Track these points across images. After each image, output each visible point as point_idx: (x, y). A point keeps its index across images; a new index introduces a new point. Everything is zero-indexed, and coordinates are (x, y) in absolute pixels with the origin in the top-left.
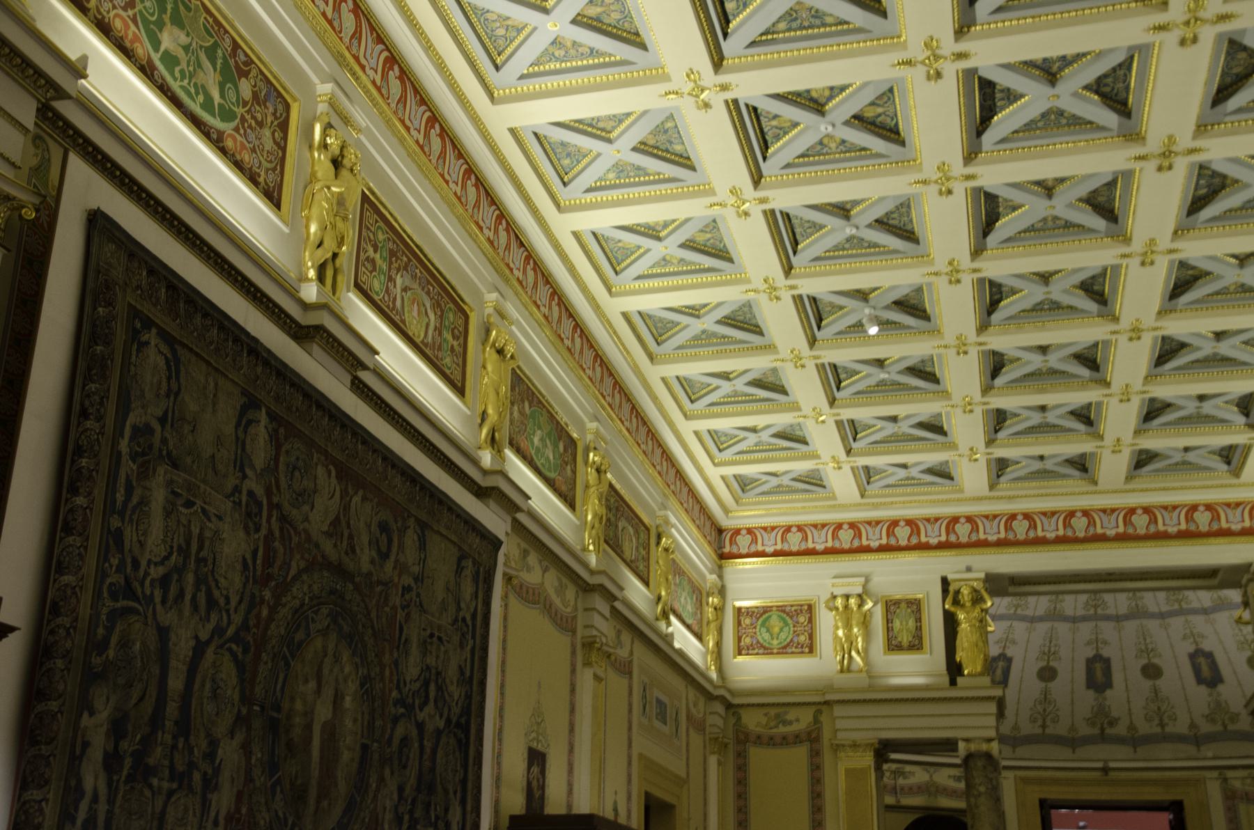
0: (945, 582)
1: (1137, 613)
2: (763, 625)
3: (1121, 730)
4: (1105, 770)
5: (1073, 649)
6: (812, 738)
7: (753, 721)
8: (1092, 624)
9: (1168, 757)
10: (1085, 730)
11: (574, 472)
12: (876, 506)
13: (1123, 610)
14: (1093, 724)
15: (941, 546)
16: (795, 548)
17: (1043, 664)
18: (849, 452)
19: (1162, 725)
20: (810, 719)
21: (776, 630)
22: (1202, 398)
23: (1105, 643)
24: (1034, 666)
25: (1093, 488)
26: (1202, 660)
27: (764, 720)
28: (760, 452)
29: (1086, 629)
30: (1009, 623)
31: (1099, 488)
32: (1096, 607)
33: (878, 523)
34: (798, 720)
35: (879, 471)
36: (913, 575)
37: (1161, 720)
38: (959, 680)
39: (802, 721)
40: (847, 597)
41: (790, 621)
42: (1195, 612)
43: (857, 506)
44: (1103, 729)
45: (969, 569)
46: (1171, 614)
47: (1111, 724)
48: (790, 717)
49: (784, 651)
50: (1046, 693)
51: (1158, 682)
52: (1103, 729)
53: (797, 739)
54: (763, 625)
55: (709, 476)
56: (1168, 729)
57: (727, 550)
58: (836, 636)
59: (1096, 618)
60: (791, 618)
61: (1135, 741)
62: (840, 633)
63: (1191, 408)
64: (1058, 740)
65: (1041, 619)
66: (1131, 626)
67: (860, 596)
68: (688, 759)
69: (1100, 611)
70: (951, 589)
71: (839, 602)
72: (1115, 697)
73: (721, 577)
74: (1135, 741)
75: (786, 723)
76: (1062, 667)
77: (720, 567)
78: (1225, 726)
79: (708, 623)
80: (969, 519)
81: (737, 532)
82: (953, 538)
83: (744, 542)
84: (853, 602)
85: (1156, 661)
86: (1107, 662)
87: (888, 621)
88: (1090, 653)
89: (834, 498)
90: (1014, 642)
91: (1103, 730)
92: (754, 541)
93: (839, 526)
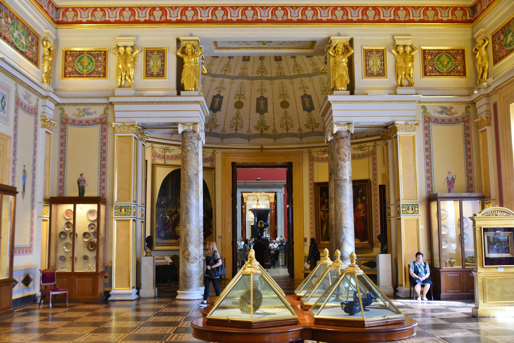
0: (178, 41)
1: (281, 76)
2: (79, 61)
3: (270, 132)
4: (262, 149)
5: (251, 93)
6: (103, 122)
7: (71, 112)
8: (260, 81)
9: (289, 143)
10: (254, 132)
13: (274, 75)
14: (258, 129)
15: (178, 22)
16: (98, 20)
17: (238, 100)
19: (287, 129)
20: (102, 112)
21: (86, 64)
24: (233, 101)
26: (306, 99)
27: (77, 112)
29: (257, 83)
30: (222, 79)
32: (262, 72)
33: (145, 8)
34: (95, 113)
36: (163, 37)
37: (287, 127)
39: (98, 112)
40: (125, 47)
41: (94, 60)
42: (305, 76)
44: (262, 131)
46: (295, 77)
47: (266, 129)
48: (90, 111)
49: (89, 75)
50: (238, 114)
51: (287, 110)
52: (262, 131)
53: (94, 122)
54: (79, 61)
56: (289, 131)
57: (60, 19)
58: (118, 68)
59: (262, 78)
60: (94, 58)
61: (275, 136)
62: (120, 66)
64: (242, 136)
65: (237, 78)
66: (277, 82)
67: (132, 47)
68: (16, 126)
69: (264, 75)
70: (183, 44)
71: (122, 50)
73: (56, 34)
74: (275, 136)
75: (88, 114)
76: (246, 102)
78: (313, 129)
81: (67, 9)
82: (184, 18)
83: (70, 15)
84: (129, 50)
87: (147, 61)
88: (259, 96)
91: (262, 131)
92: (76, 15)
93: (124, 9)
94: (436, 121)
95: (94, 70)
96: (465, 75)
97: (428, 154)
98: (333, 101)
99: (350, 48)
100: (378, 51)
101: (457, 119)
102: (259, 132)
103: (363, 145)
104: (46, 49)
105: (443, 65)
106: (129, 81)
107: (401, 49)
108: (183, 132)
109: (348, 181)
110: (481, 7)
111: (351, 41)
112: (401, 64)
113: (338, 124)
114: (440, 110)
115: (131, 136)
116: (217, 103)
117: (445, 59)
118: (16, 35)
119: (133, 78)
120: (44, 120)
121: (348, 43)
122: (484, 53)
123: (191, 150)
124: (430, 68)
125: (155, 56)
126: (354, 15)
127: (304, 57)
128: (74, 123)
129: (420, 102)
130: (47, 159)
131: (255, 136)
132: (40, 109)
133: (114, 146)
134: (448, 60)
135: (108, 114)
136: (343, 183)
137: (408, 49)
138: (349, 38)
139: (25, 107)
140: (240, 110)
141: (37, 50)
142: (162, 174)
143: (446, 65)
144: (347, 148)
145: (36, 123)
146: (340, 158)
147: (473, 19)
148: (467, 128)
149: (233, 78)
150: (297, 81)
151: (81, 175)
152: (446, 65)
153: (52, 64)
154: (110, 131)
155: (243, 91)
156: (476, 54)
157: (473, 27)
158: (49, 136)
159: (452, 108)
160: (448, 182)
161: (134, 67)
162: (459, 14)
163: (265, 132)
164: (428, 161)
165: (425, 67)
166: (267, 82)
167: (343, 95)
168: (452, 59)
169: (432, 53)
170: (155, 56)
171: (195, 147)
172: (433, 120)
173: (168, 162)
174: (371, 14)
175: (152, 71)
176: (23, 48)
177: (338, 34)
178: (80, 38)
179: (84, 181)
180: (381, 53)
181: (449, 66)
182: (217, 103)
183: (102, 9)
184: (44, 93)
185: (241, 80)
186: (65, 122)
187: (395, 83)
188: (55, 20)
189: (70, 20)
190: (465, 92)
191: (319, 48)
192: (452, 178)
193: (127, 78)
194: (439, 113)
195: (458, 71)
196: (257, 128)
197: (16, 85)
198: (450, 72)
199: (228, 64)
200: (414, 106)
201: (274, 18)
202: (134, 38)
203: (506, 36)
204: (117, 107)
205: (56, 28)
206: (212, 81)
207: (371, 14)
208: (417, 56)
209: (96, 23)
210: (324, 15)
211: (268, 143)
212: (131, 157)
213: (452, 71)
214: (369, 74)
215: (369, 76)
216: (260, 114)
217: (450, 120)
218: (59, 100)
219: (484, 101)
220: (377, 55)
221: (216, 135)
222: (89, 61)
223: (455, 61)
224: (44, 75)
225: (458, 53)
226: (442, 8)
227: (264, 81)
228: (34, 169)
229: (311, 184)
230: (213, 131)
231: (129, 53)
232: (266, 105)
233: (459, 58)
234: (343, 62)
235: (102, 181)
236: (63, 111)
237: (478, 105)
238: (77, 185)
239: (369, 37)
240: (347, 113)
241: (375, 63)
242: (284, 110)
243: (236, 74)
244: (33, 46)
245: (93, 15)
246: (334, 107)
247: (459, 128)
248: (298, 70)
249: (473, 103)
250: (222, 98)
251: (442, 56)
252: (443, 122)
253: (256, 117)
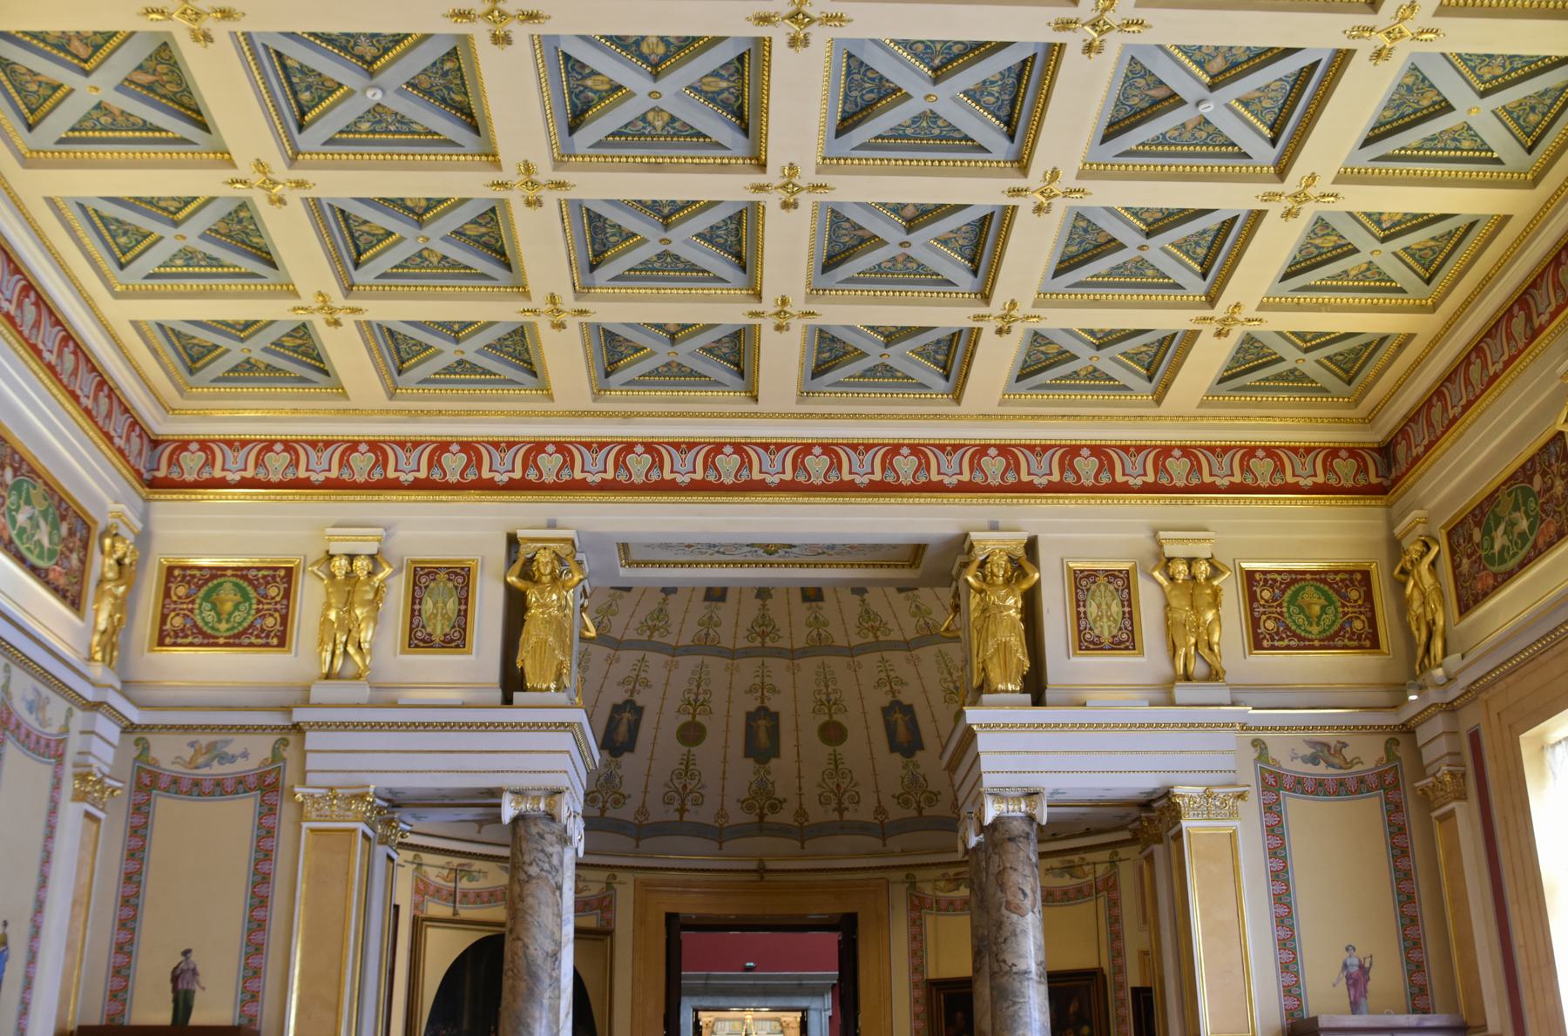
0: (513, 541)
1: (820, 647)
2: (206, 598)
3: (786, 817)
4: (762, 871)
5: (730, 694)
6: (267, 787)
7: (169, 754)
10: (738, 816)
12: (414, 416)
13: (799, 643)
14: (750, 808)
15: (513, 486)
16: (275, 478)
17: (689, 718)
18: (349, 289)
19: (841, 810)
20: (268, 754)
21: (228, 606)
23: (774, 690)
24: (674, 721)
25: (752, 407)
26: (898, 716)
27: (188, 753)
29: (748, 666)
31: (761, 407)
32: (763, 635)
33: (416, 444)
34: (245, 755)
36: (467, 529)
37: (840, 803)
38: (518, 696)
39: (254, 753)
40: (351, 558)
41: (252, 594)
42: (894, 646)
46: (864, 649)
48: (230, 750)
50: (687, 762)
51: (839, 749)
53: (240, 785)
54: (206, 598)
56: (847, 816)
57: (161, 474)
58: (325, 621)
60: (256, 588)
61: (803, 832)
62: (333, 615)
64: (701, 830)
65: (687, 651)
66: (809, 665)
67: (372, 557)
69: (769, 643)
70: (525, 551)
71: (340, 565)
72: (782, 769)
73: (145, 518)
75: (224, 758)
78: (920, 810)
79: (102, 581)
81: (183, 445)
82: (532, 475)
83: (192, 463)
84: (361, 565)
85: (836, 718)
86: (774, 717)
87: (415, 600)
88: (753, 706)
90: (647, 685)
91: (762, 816)
92: (210, 462)
94: (1299, 785)
95: (251, 625)
96: (1375, 645)
97: (1279, 888)
98: (980, 725)
99: (1028, 566)
100: (1111, 575)
101: (1361, 781)
102: (753, 818)
103: (1075, 858)
104: (111, 562)
105: (1308, 618)
106: (357, 659)
107: (1181, 570)
108: (516, 820)
109: (1034, 975)
110: (1409, 448)
111: (1031, 546)
112: (1183, 612)
113: (998, 796)
114: (1309, 751)
115: (354, 830)
116: (623, 728)
117: (1313, 600)
118: (22, 518)
119: (370, 651)
120: (83, 778)
121: (1020, 552)
122: (1428, 580)
123: (538, 877)
124: (1270, 625)
125: (442, 584)
127: (892, 591)
128: (176, 786)
129: (1245, 727)
130: (82, 902)
131: (740, 831)
132: (74, 743)
133: (298, 859)
134: (1323, 601)
135: (284, 760)
136: (1017, 984)
137: (1203, 569)
138: (1023, 536)
139: (28, 735)
140: (694, 750)
141: (83, 562)
142: (443, 949)
143: (1319, 617)
144: (1027, 871)
145: (57, 786)
146: (1008, 903)
147: (1386, 483)
148: (1394, 809)
149: (675, 651)
150: (870, 661)
151: (186, 953)
152: (1319, 617)
153: (125, 606)
154: (287, 812)
155: (705, 692)
156: (1404, 585)
157: (1389, 506)
158: (94, 826)
159: (1345, 745)
160: (1348, 977)
161: (375, 616)
162: (1345, 469)
163: (771, 818)
164: (1283, 911)
165: (1255, 623)
166: (777, 666)
167: (1012, 705)
168: (1335, 597)
169: (1275, 581)
170: (442, 584)
171: (552, 866)
172: (1288, 782)
173: (465, 913)
174: (1087, 467)
175: (429, 630)
176: (40, 556)
177: (992, 526)
178: (215, 530)
179: (194, 972)
180: (1122, 582)
181: (1327, 619)
182: (623, 728)
183: (289, 446)
184: (89, 694)
185: (698, 659)
186: (148, 783)
187: (1166, 668)
188: (146, 476)
190: (1381, 697)
191: (938, 567)
192: (1361, 967)
193: (351, 650)
194: (1305, 760)
195: (1353, 633)
196: (747, 805)
197: (7, 669)
198: (1331, 638)
199: (661, 610)
200: (1228, 739)
201: (802, 478)
202: (380, 531)
203: (1488, 532)
204: (313, 739)
205: (147, 500)
206: (610, 661)
207: (1087, 467)
208: (1231, 590)
209: (268, 485)
210: (949, 470)
211: (780, 854)
212: (347, 897)
213: (1336, 634)
214: (1086, 642)
215: (1088, 649)
216: (758, 761)
217: (1341, 783)
218: (135, 716)
219: (1439, 724)
220: (1111, 587)
221: (619, 827)
222: (238, 598)
223: (1343, 606)
224: (96, 638)
225: (1352, 581)
226: (1295, 450)
227: (768, 661)
228: (36, 933)
229: (915, 986)
230: (610, 813)
231: (362, 575)
232: (774, 732)
233: (1354, 595)
234: (1010, 608)
235: (252, 973)
236: (145, 747)
237: (1423, 734)
238: (169, 986)
239: (1082, 533)
240: (1025, 760)
241: (1104, 611)
242: (830, 749)
243: (686, 640)
244: (71, 551)
245: (259, 463)
246: (984, 742)
247: (1370, 809)
248: (874, 629)
249: (1408, 730)
250: (639, 711)
251: (1303, 588)
252: (1319, 788)
253: (744, 771)
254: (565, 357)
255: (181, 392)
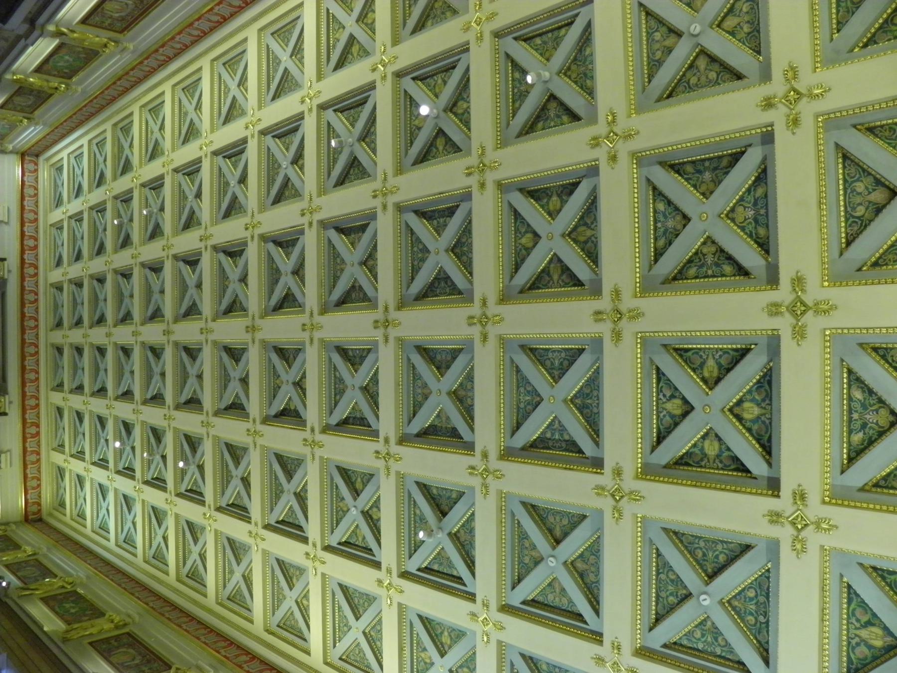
11: (54, 76)
12: (45, 232)
22: (83, 369)
25: (49, 329)
28: (73, 176)
35: (62, 232)
43: (46, 221)
45: (9, 271)
55: (63, 151)
57: (27, 158)
63: (80, 365)
73: (11, 152)
77: (17, 153)
80: (36, 275)
81: (36, 164)
83: (31, 167)
89: (51, 211)
92: (30, 172)
126: (30, 416)
138: (7, 411)
157: (21, 522)
162: (34, 509)
174: (33, 430)
189: (25, 166)
207: (33, 430)
210: (30, 389)
254: (56, 276)
255: (52, 165)
